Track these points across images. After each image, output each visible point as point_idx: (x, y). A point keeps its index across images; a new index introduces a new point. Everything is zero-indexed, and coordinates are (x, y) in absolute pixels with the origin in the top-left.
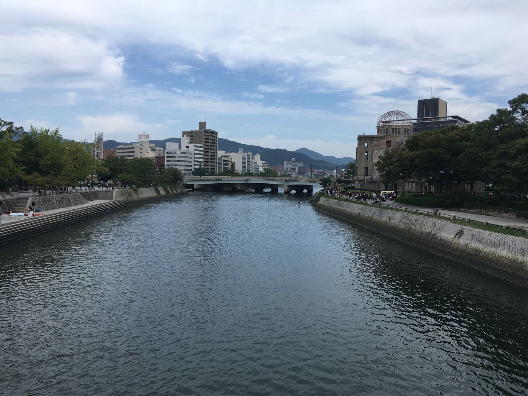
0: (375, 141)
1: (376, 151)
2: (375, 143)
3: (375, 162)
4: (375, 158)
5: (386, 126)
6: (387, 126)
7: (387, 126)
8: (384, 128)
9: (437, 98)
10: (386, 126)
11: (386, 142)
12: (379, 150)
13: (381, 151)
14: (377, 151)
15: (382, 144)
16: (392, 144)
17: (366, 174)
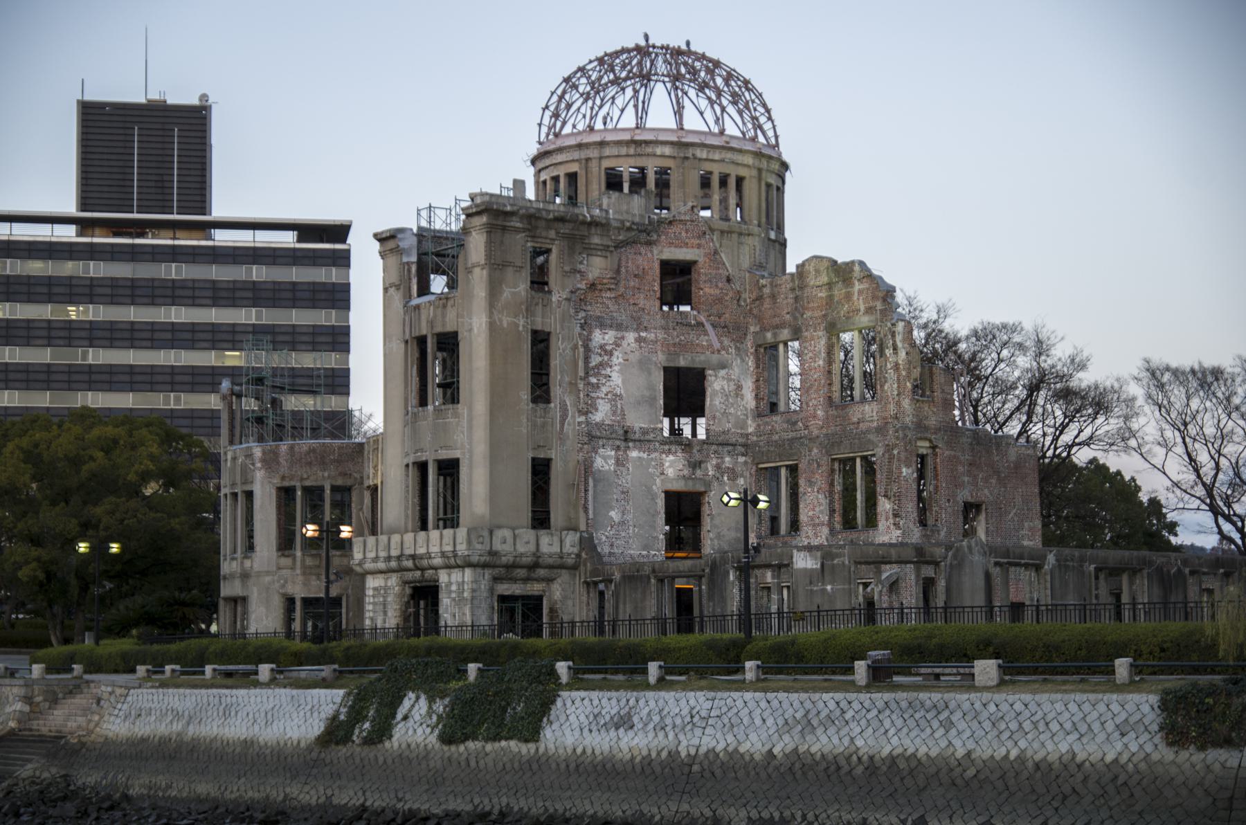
0: (589, 250)
1: (598, 337)
2: (596, 267)
3: (598, 417)
4: (597, 387)
5: (659, 151)
6: (667, 150)
7: (667, 150)
8: (641, 162)
9: (195, 101)
10: (659, 150)
11: (657, 266)
12: (619, 327)
13: (631, 337)
14: (610, 336)
15: (633, 283)
16: (704, 289)
17: (541, 520)
